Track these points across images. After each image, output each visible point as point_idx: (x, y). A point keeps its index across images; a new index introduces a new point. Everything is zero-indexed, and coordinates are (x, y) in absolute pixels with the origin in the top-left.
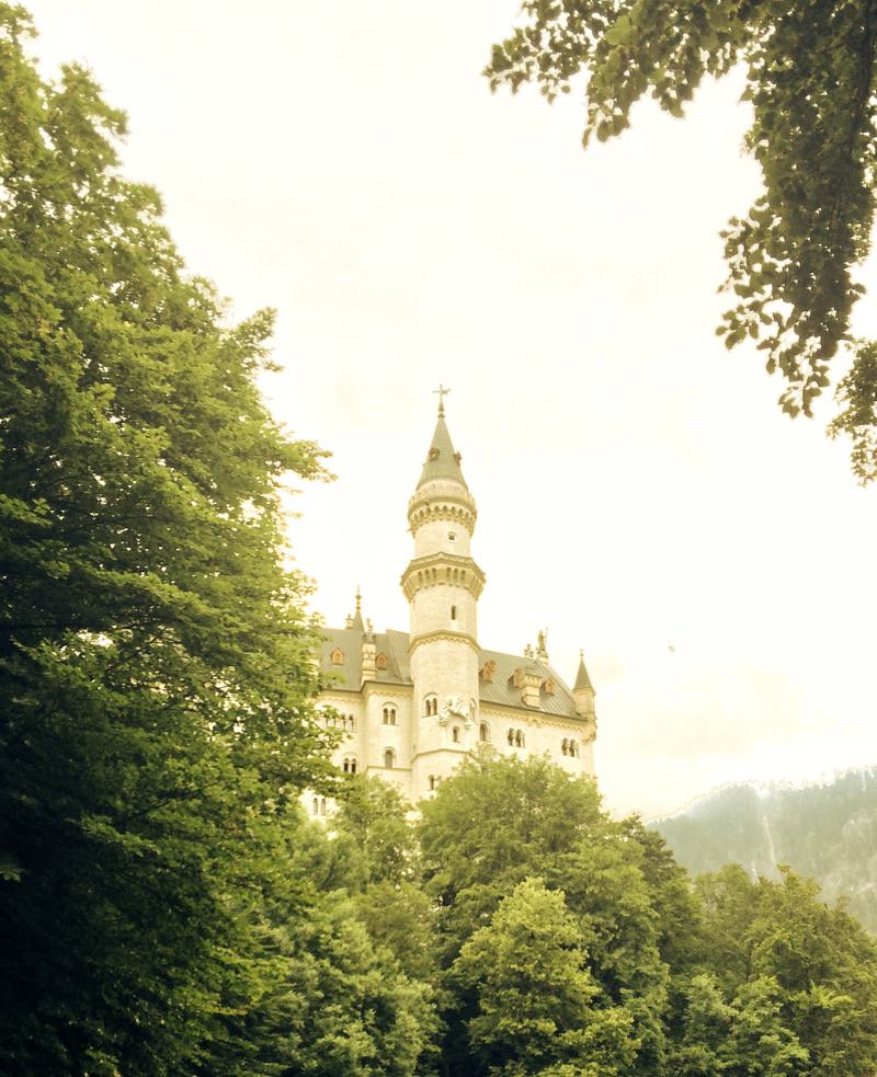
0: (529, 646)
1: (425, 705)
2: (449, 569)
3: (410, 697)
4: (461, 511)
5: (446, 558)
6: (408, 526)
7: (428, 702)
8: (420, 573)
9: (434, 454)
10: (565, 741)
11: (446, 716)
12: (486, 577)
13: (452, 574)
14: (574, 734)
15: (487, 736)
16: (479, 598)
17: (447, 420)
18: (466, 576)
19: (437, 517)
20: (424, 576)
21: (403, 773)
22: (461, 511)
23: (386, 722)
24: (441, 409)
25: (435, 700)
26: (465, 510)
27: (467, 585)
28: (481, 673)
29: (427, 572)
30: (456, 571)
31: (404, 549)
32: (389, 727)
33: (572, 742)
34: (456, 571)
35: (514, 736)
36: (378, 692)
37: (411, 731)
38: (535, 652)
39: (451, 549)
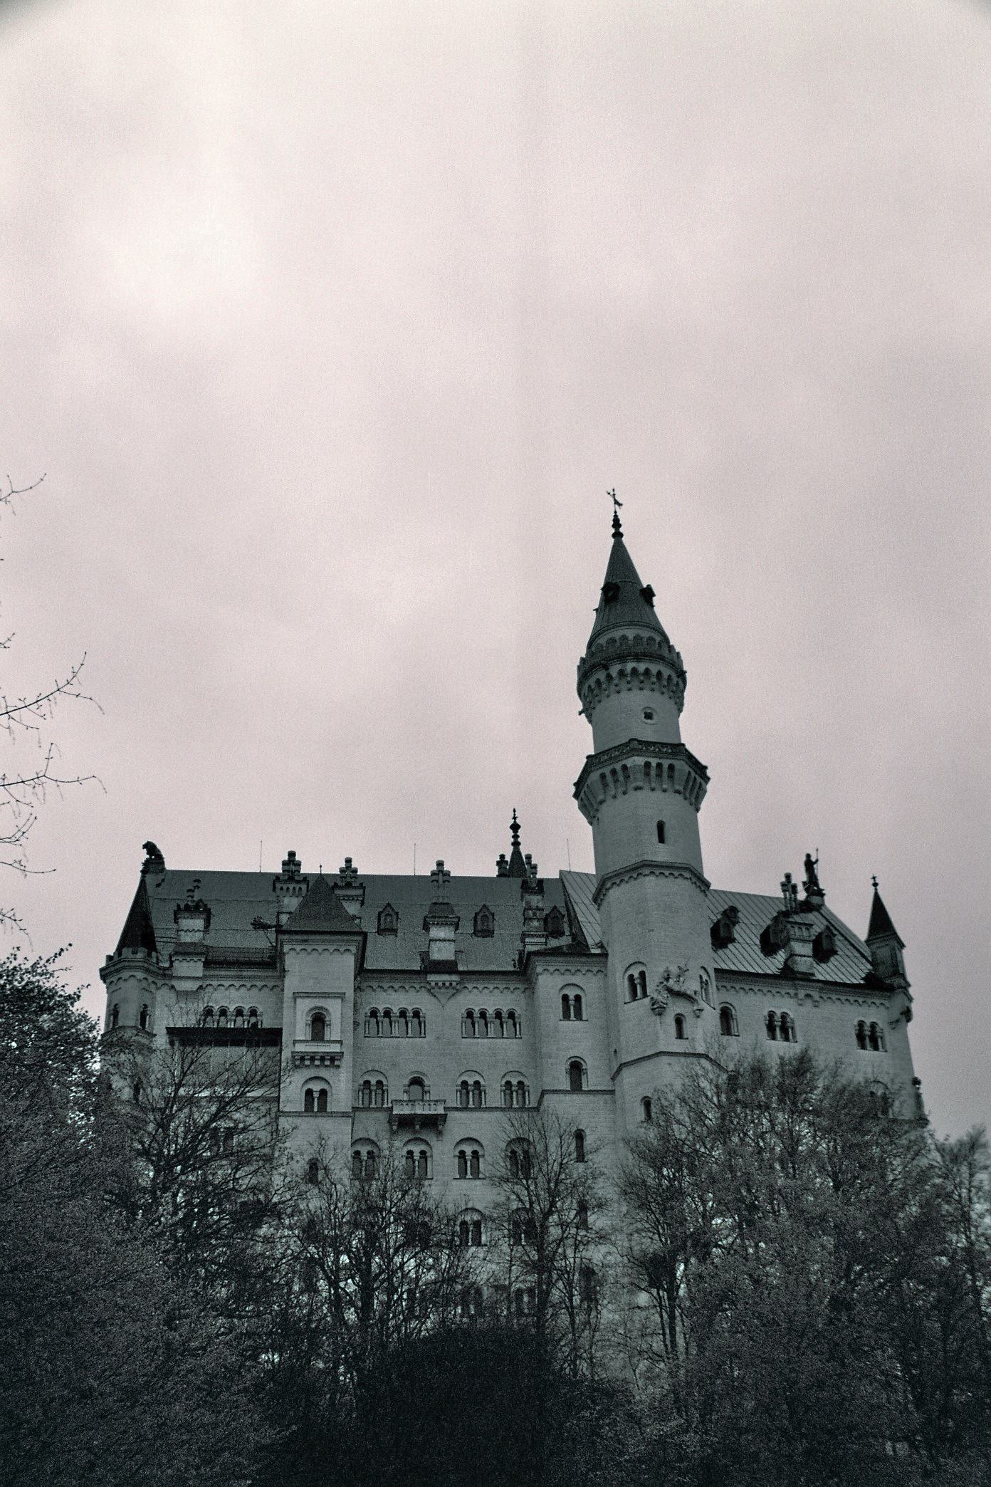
0: (788, 877)
2: (648, 765)
4: (659, 673)
7: (631, 977)
8: (603, 776)
10: (861, 1024)
11: (662, 997)
12: (709, 773)
13: (653, 772)
14: (873, 1013)
15: (733, 1024)
16: (704, 805)
18: (677, 774)
19: (624, 685)
20: (609, 778)
21: (600, 1099)
22: (659, 673)
23: (566, 1016)
25: (642, 974)
26: (667, 672)
27: (677, 787)
28: (715, 932)
29: (614, 772)
30: (659, 766)
31: (580, 740)
32: (573, 1024)
33: (873, 1025)
36: (551, 969)
37: (610, 1028)
38: (800, 888)
39: (648, 732)
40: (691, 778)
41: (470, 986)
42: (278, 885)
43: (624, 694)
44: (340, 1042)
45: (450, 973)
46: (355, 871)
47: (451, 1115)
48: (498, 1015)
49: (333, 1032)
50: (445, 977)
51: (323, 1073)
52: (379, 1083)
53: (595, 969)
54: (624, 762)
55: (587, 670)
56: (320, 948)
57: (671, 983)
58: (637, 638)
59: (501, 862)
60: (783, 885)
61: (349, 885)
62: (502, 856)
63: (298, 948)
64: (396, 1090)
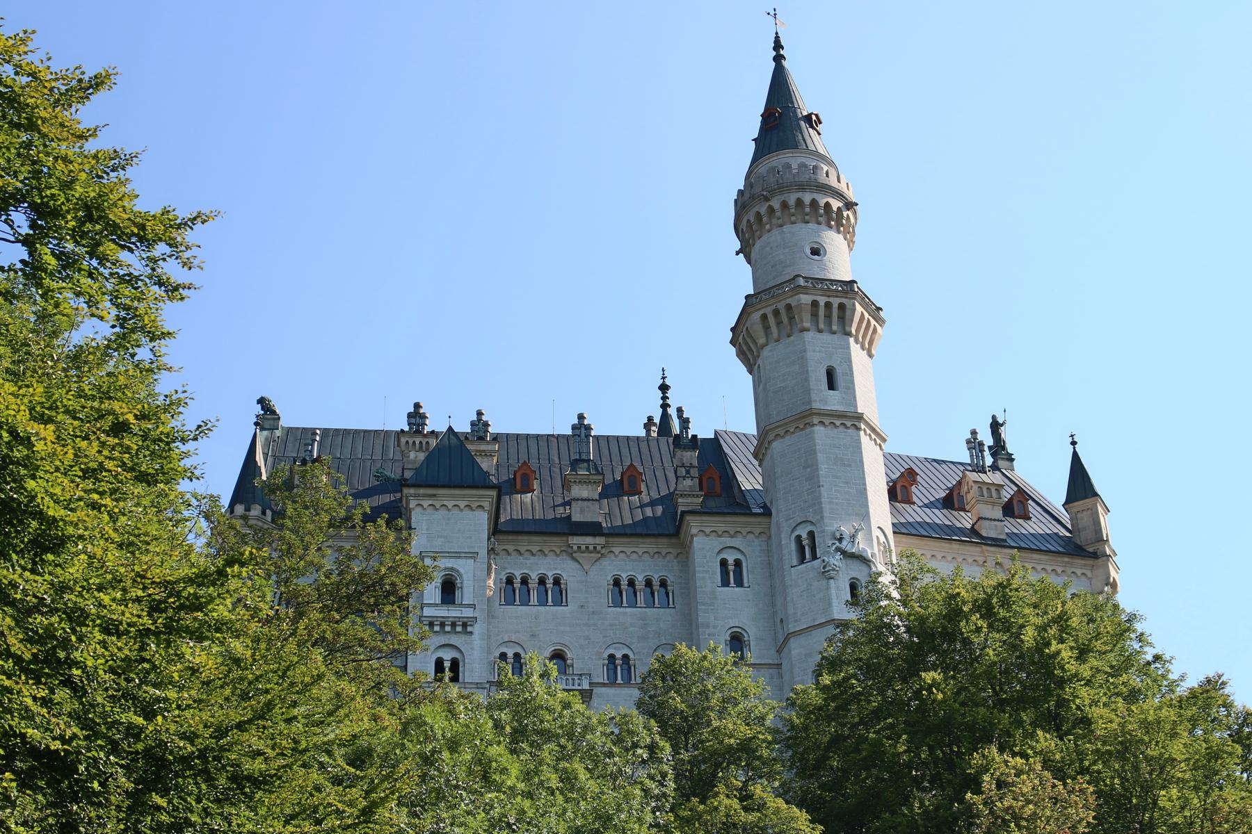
0: (974, 433)
1: (793, 546)
2: (815, 304)
3: (766, 534)
4: (828, 205)
6: (738, 246)
7: (799, 537)
9: (769, 118)
11: (836, 560)
17: (785, 63)
18: (848, 313)
23: (725, 583)
24: (778, 46)
25: (811, 535)
29: (776, 313)
32: (733, 591)
37: (774, 597)
41: (616, 550)
42: (403, 440)
43: (786, 228)
44: (473, 606)
45: (594, 535)
46: (486, 425)
47: (596, 690)
48: (649, 583)
49: (466, 594)
50: (589, 540)
51: (454, 640)
52: (517, 656)
53: (757, 531)
54: (788, 301)
55: (743, 203)
56: (450, 504)
57: (844, 543)
60: (968, 442)
61: (481, 439)
62: (650, 419)
63: (426, 503)
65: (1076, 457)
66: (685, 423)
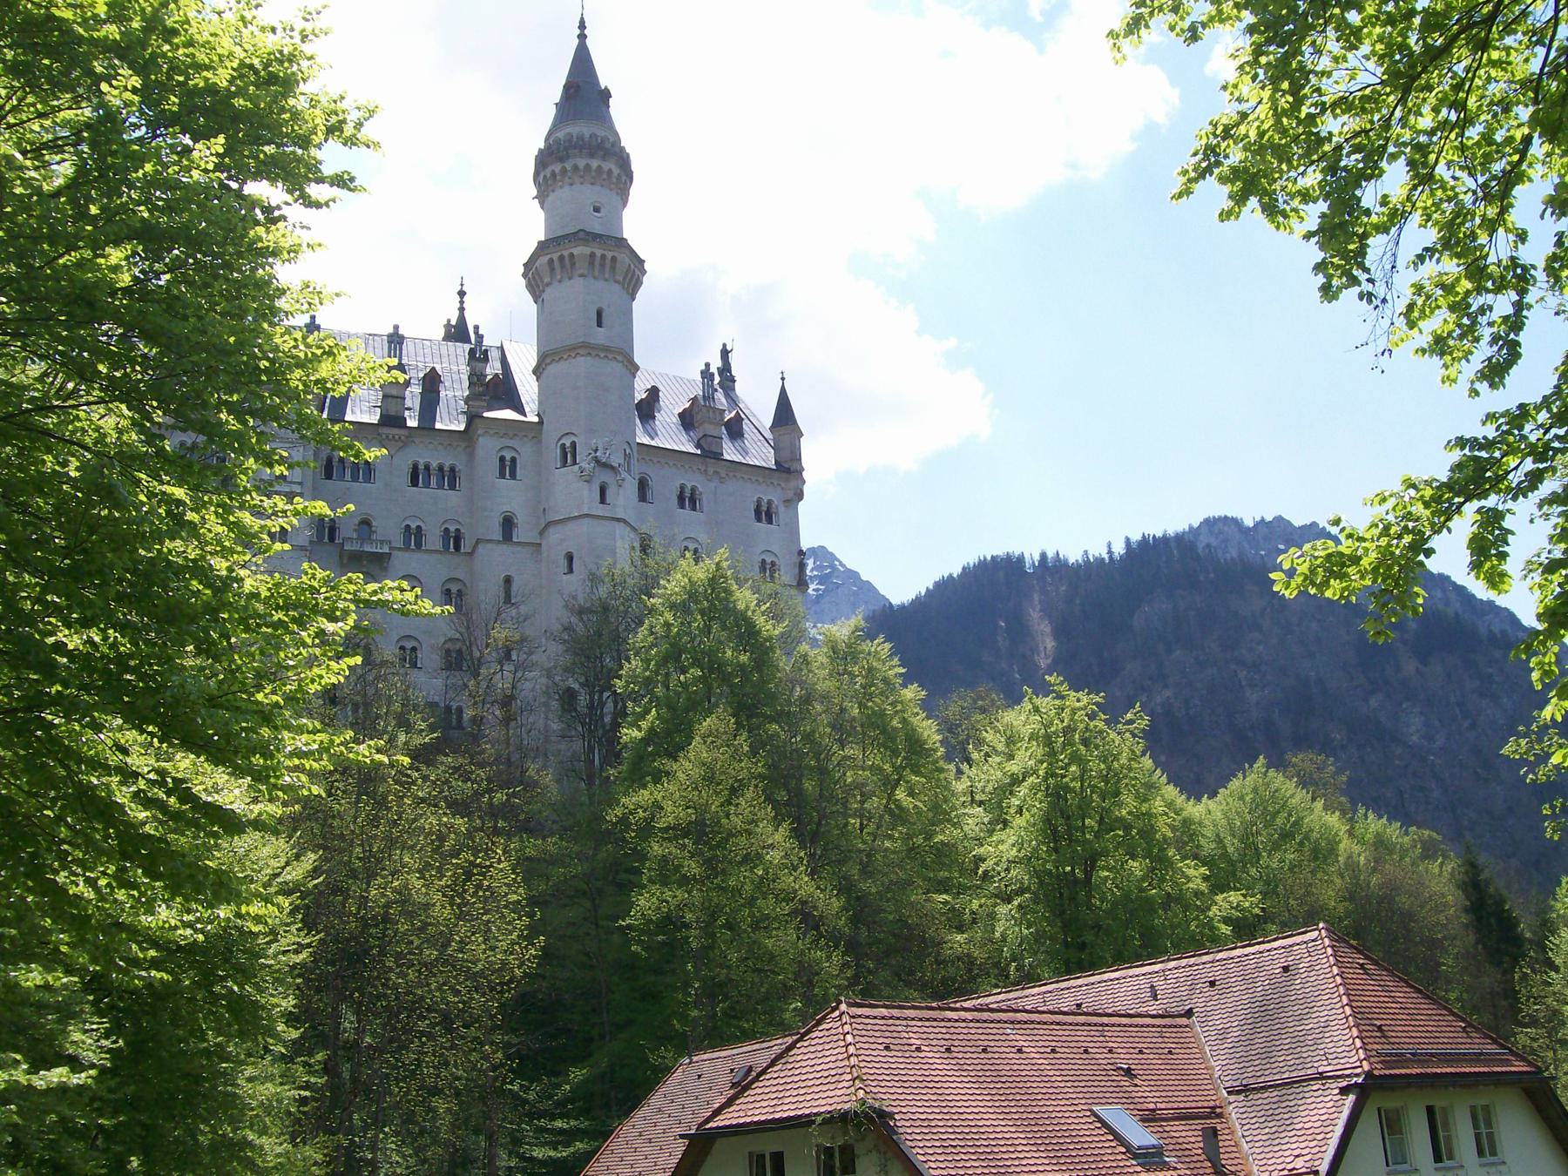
0: (707, 365)
2: (592, 255)
4: (610, 171)
5: (594, 237)
6: (534, 192)
8: (551, 261)
19: (577, 179)
23: (502, 476)
25: (574, 445)
26: (616, 171)
30: (603, 256)
31: (529, 226)
32: (507, 483)
33: (770, 502)
34: (603, 256)
35: (688, 494)
40: (626, 270)
43: (577, 187)
44: (300, 483)
47: (395, 553)
48: (441, 468)
50: (395, 431)
55: (543, 160)
58: (593, 136)
59: (448, 325)
64: (347, 531)
65: (783, 388)
66: (480, 337)
